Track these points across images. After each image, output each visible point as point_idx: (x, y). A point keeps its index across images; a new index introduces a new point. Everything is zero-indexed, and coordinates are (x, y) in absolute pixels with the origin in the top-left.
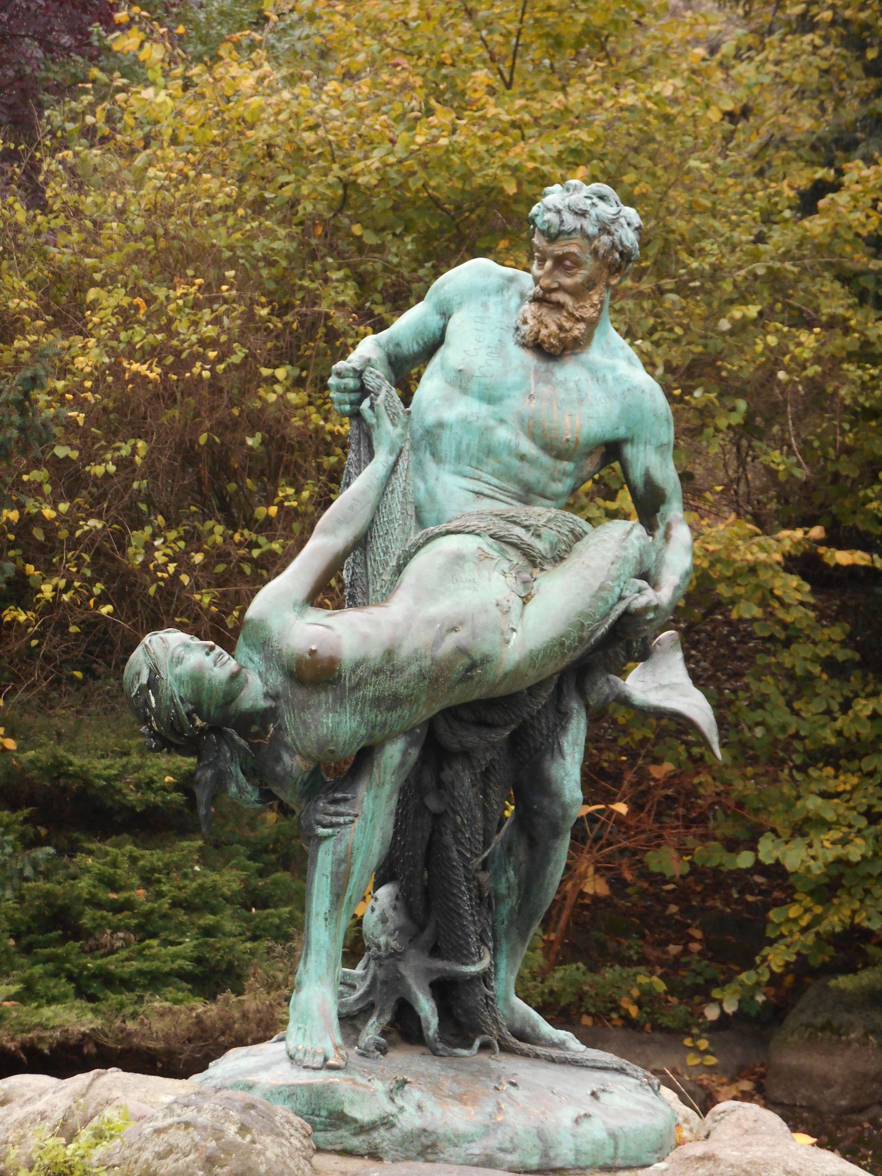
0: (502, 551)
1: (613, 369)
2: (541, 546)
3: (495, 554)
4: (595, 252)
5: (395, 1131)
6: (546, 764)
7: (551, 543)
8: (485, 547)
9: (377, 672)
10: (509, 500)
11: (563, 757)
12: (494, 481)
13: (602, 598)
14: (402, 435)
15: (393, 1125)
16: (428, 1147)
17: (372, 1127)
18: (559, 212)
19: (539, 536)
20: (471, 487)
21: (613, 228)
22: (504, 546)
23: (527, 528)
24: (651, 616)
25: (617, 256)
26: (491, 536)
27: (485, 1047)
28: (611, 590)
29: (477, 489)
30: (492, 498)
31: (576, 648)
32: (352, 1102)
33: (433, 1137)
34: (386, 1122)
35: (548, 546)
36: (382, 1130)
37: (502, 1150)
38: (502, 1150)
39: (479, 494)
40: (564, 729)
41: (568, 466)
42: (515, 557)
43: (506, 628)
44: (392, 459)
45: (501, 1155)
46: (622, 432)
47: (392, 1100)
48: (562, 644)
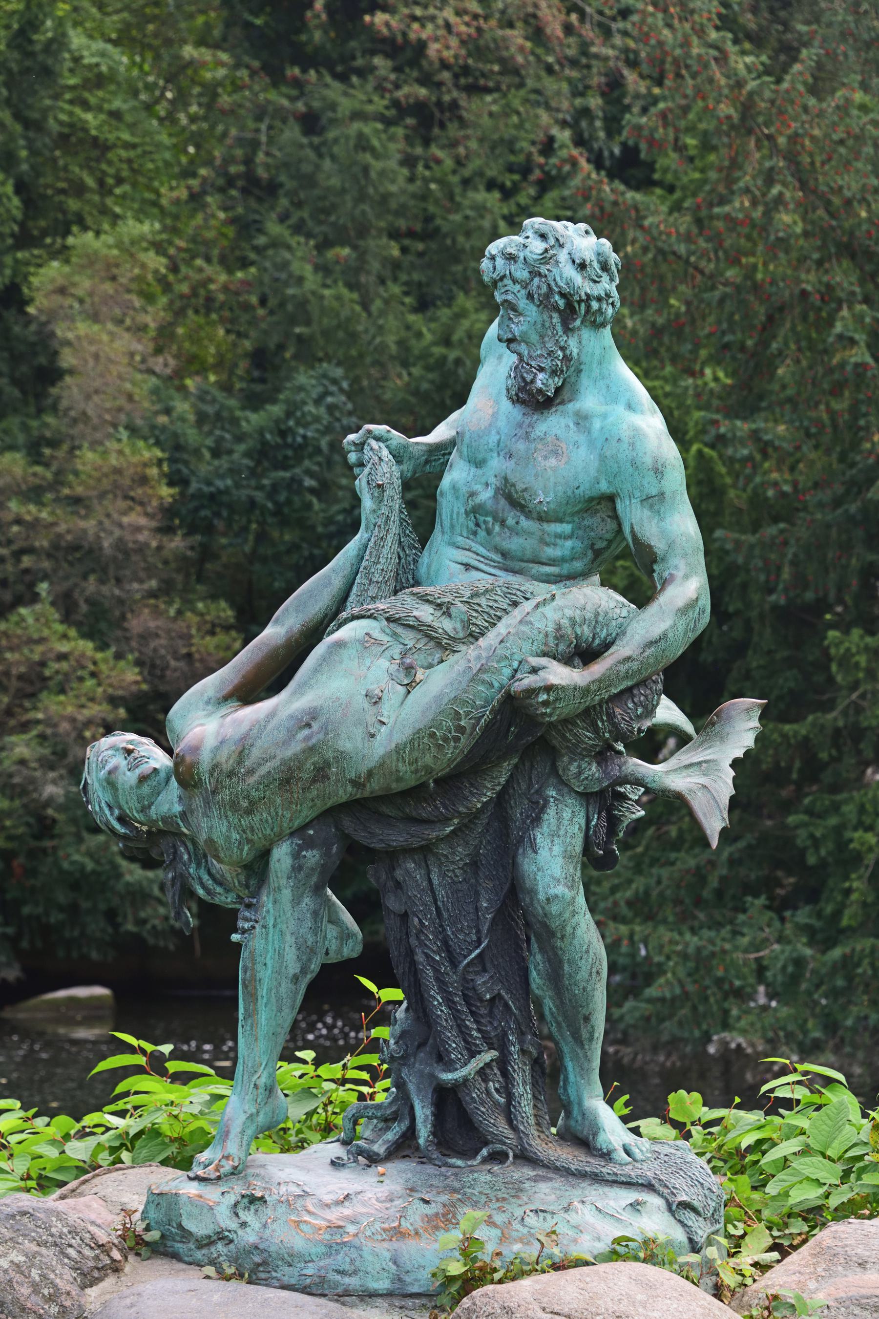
0: (395, 635)
1: (605, 416)
2: (447, 625)
3: (385, 638)
4: (530, 296)
5: (232, 1246)
6: (520, 858)
7: (462, 621)
8: (377, 634)
9: (231, 774)
10: (492, 571)
11: (536, 852)
12: (482, 550)
13: (483, 682)
14: (374, 511)
15: (231, 1241)
16: (259, 1265)
17: (206, 1242)
18: (493, 258)
19: (448, 614)
20: (460, 560)
21: (543, 269)
22: (399, 630)
23: (439, 606)
24: (543, 697)
25: (557, 297)
26: (388, 619)
27: (498, 1157)
28: (498, 671)
29: (465, 560)
30: (477, 569)
31: (457, 739)
32: (190, 1215)
33: (265, 1255)
34: (221, 1236)
35: (459, 626)
36: (220, 1246)
37: (339, 1272)
38: (339, 1272)
39: (468, 567)
40: (537, 820)
41: (566, 528)
42: (409, 638)
43: (371, 719)
44: (366, 535)
45: (338, 1277)
46: (604, 487)
47: (237, 1215)
48: (433, 735)
